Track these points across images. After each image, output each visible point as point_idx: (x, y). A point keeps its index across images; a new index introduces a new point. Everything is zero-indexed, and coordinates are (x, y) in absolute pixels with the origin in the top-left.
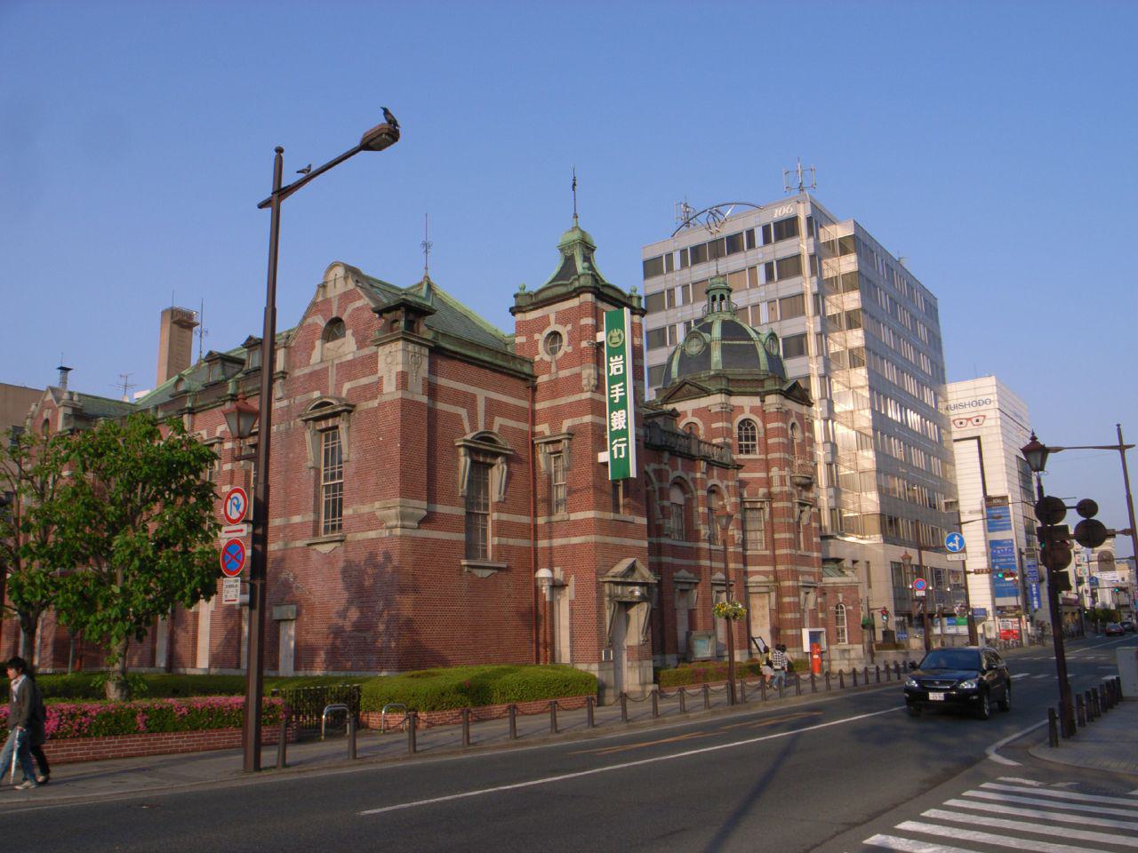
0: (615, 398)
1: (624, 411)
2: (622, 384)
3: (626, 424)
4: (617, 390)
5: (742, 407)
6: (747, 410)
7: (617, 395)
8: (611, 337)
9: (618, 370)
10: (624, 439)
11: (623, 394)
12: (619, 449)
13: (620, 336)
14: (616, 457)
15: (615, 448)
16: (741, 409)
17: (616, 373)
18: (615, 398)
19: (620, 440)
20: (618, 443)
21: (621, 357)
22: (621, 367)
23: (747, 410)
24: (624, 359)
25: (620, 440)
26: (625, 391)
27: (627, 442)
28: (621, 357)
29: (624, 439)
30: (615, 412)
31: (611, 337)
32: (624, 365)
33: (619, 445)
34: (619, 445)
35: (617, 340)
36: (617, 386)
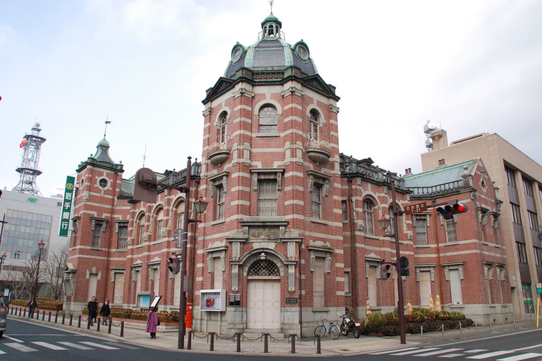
0: (66, 207)
1: (69, 213)
2: (70, 203)
3: (69, 217)
4: (67, 205)
5: (264, 94)
6: (268, 96)
7: (67, 207)
8: (68, 186)
9: (69, 198)
10: (67, 223)
11: (70, 207)
12: (65, 226)
13: (72, 186)
14: (63, 228)
15: (63, 225)
16: (263, 96)
17: (68, 199)
18: (66, 207)
19: (66, 223)
20: (65, 223)
21: (71, 194)
22: (70, 197)
23: (268, 96)
24: (72, 195)
25: (66, 223)
26: (71, 206)
27: (68, 224)
28: (71, 194)
29: (67, 223)
30: (65, 212)
31: (68, 186)
32: (72, 197)
33: (65, 224)
34: (65, 224)
35: (70, 187)
36: (68, 203)
